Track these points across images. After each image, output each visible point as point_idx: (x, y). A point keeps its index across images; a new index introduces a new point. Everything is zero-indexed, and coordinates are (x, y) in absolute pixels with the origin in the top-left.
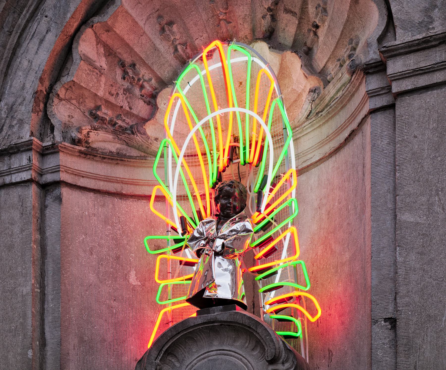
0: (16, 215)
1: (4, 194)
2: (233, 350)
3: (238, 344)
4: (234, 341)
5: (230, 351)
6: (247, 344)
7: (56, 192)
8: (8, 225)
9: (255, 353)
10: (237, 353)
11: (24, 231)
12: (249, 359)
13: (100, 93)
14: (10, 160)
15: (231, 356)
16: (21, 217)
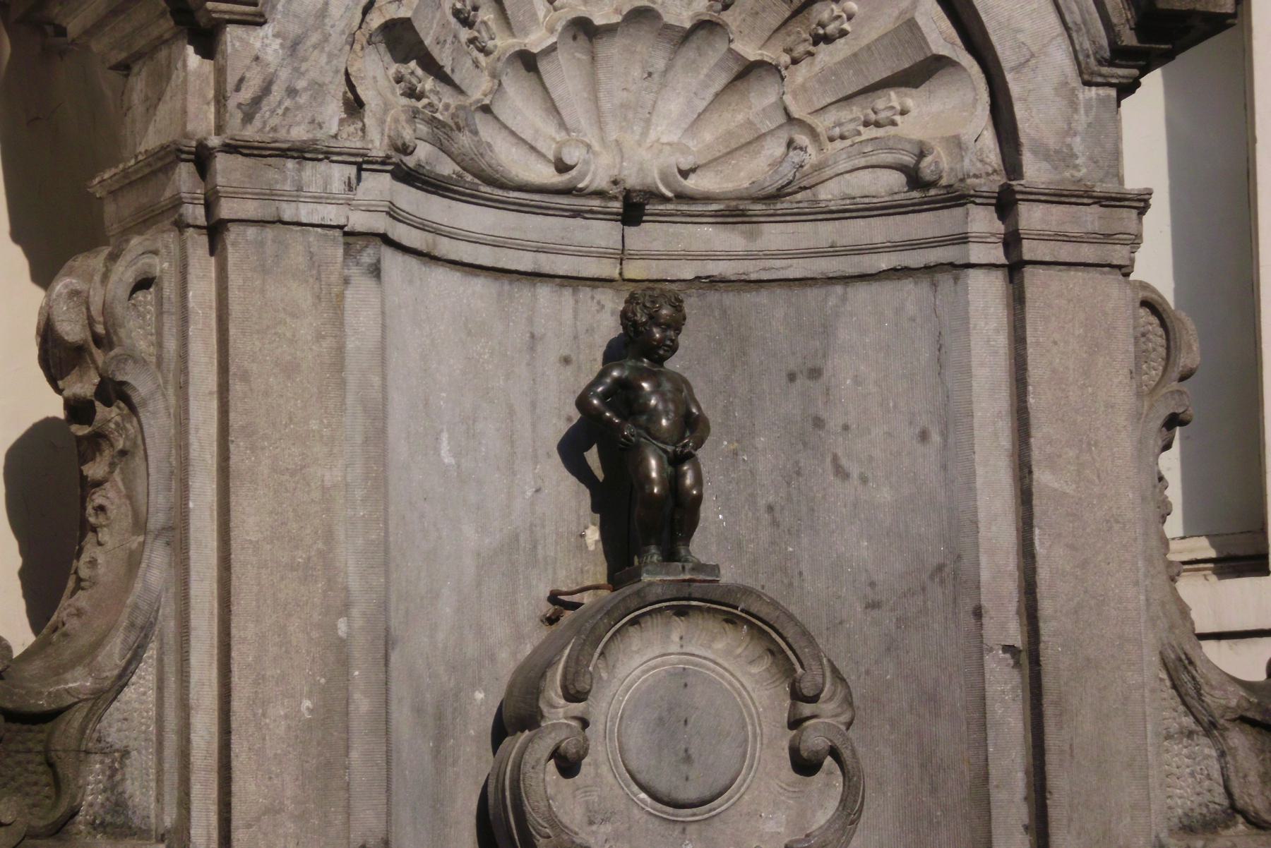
0: (302, 295)
1: (274, 241)
2: (712, 656)
3: (720, 645)
4: (713, 639)
5: (705, 658)
6: (739, 651)
7: (367, 258)
8: (282, 315)
9: (755, 670)
10: (720, 666)
11: (324, 337)
12: (743, 680)
13: (427, 42)
14: (299, 171)
15: (708, 669)
16: (314, 305)
